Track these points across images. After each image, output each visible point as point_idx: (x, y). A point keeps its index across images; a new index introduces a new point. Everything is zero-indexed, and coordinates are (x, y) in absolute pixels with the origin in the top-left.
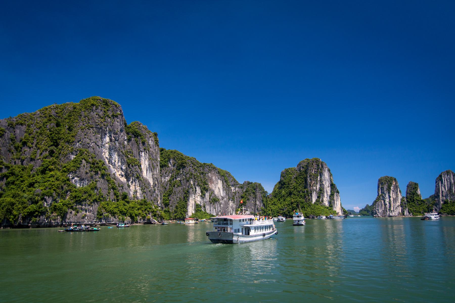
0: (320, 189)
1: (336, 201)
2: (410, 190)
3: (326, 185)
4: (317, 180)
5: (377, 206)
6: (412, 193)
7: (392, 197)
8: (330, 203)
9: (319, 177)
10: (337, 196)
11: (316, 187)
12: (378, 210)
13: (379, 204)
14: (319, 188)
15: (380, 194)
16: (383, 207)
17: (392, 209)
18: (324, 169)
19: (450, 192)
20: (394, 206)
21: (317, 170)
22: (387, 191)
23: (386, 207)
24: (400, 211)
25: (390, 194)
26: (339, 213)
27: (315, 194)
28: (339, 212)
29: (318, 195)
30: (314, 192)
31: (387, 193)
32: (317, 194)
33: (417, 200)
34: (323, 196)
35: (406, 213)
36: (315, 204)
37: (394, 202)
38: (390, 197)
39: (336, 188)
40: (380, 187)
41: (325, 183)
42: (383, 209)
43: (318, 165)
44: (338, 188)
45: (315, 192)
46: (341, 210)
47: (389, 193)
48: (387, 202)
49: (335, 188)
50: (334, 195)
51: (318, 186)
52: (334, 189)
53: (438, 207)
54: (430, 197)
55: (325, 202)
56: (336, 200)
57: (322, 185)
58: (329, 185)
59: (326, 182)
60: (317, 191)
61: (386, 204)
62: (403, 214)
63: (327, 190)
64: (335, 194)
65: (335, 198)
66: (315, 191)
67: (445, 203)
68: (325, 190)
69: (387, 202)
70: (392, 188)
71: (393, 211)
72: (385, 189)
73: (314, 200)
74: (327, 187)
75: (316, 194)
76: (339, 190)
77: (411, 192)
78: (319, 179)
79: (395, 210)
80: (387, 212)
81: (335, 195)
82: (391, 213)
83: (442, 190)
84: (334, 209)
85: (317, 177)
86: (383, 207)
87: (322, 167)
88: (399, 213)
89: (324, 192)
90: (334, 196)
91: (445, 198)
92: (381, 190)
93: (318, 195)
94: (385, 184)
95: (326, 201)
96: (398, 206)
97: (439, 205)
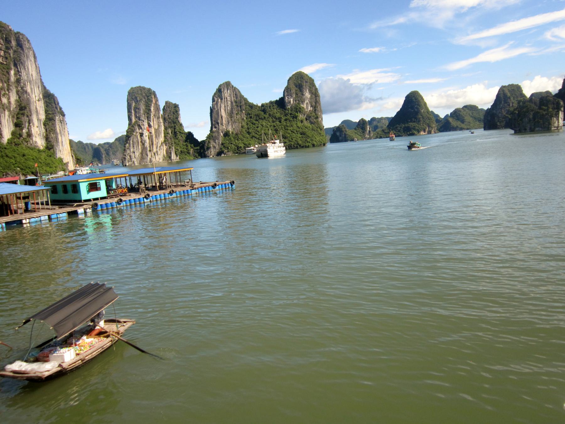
0: (20, 105)
1: (61, 136)
2: (168, 116)
3: (34, 96)
4: (9, 79)
5: (131, 146)
6: (173, 122)
7: (153, 127)
8: (47, 138)
9: (12, 72)
10: (61, 123)
11: (9, 99)
12: (134, 152)
13: (135, 140)
14: (16, 100)
15: (134, 120)
16: (140, 147)
17: (155, 150)
18: (26, 51)
19: (232, 117)
20: (157, 143)
21: (5, 52)
22: (145, 115)
23: (144, 146)
24: (165, 153)
25: (150, 121)
26: (68, 163)
27: (7, 117)
28: (69, 160)
29: (15, 121)
30: (5, 110)
31: (145, 119)
32: (13, 117)
33: (180, 133)
34: (29, 123)
35: (173, 156)
36: (11, 143)
37: (156, 137)
38: (150, 126)
39: (58, 104)
40: (133, 108)
41: (31, 89)
42: (140, 151)
43: (7, 41)
44: (63, 103)
45: (7, 113)
46: (72, 156)
47: (149, 118)
48: (146, 136)
49: (55, 105)
50: (55, 121)
51: (14, 97)
52: (54, 105)
53: (217, 142)
54: (116, 140)
55: (36, 137)
56: (61, 133)
57: (22, 93)
59: (33, 87)
60: (12, 109)
61: (145, 141)
62: (170, 157)
63: (38, 108)
64: (57, 118)
65: (57, 126)
66: (6, 110)
67: (226, 134)
68: (33, 108)
69: (146, 136)
70: (152, 109)
71: (156, 154)
72: (142, 112)
74: (37, 101)
75: (9, 116)
76: (64, 110)
77: (170, 118)
78: (13, 79)
79: (159, 153)
80: (147, 155)
81: (56, 120)
82: (154, 157)
83: (221, 115)
84: (59, 155)
85: (8, 73)
86: (140, 147)
87: (20, 45)
88: (164, 156)
89: (30, 111)
90: (56, 122)
91: (226, 127)
92: (136, 112)
93: (15, 121)
94: (141, 100)
95: (37, 136)
96: (162, 143)
97: (218, 139)
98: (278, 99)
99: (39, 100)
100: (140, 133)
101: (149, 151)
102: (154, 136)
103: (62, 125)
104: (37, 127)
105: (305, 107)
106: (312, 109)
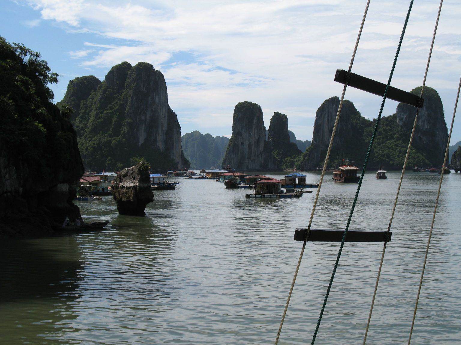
3: (161, 114)
26: (178, 163)
41: (160, 109)
45: (143, 126)
58: (166, 114)
60: (147, 123)
64: (175, 130)
73: (141, 141)
74: (163, 118)
98: (392, 115)
99: (164, 117)
100: (241, 143)
101: (247, 158)
102: (253, 146)
103: (177, 135)
104: (161, 136)
105: (420, 125)
106: (428, 127)
